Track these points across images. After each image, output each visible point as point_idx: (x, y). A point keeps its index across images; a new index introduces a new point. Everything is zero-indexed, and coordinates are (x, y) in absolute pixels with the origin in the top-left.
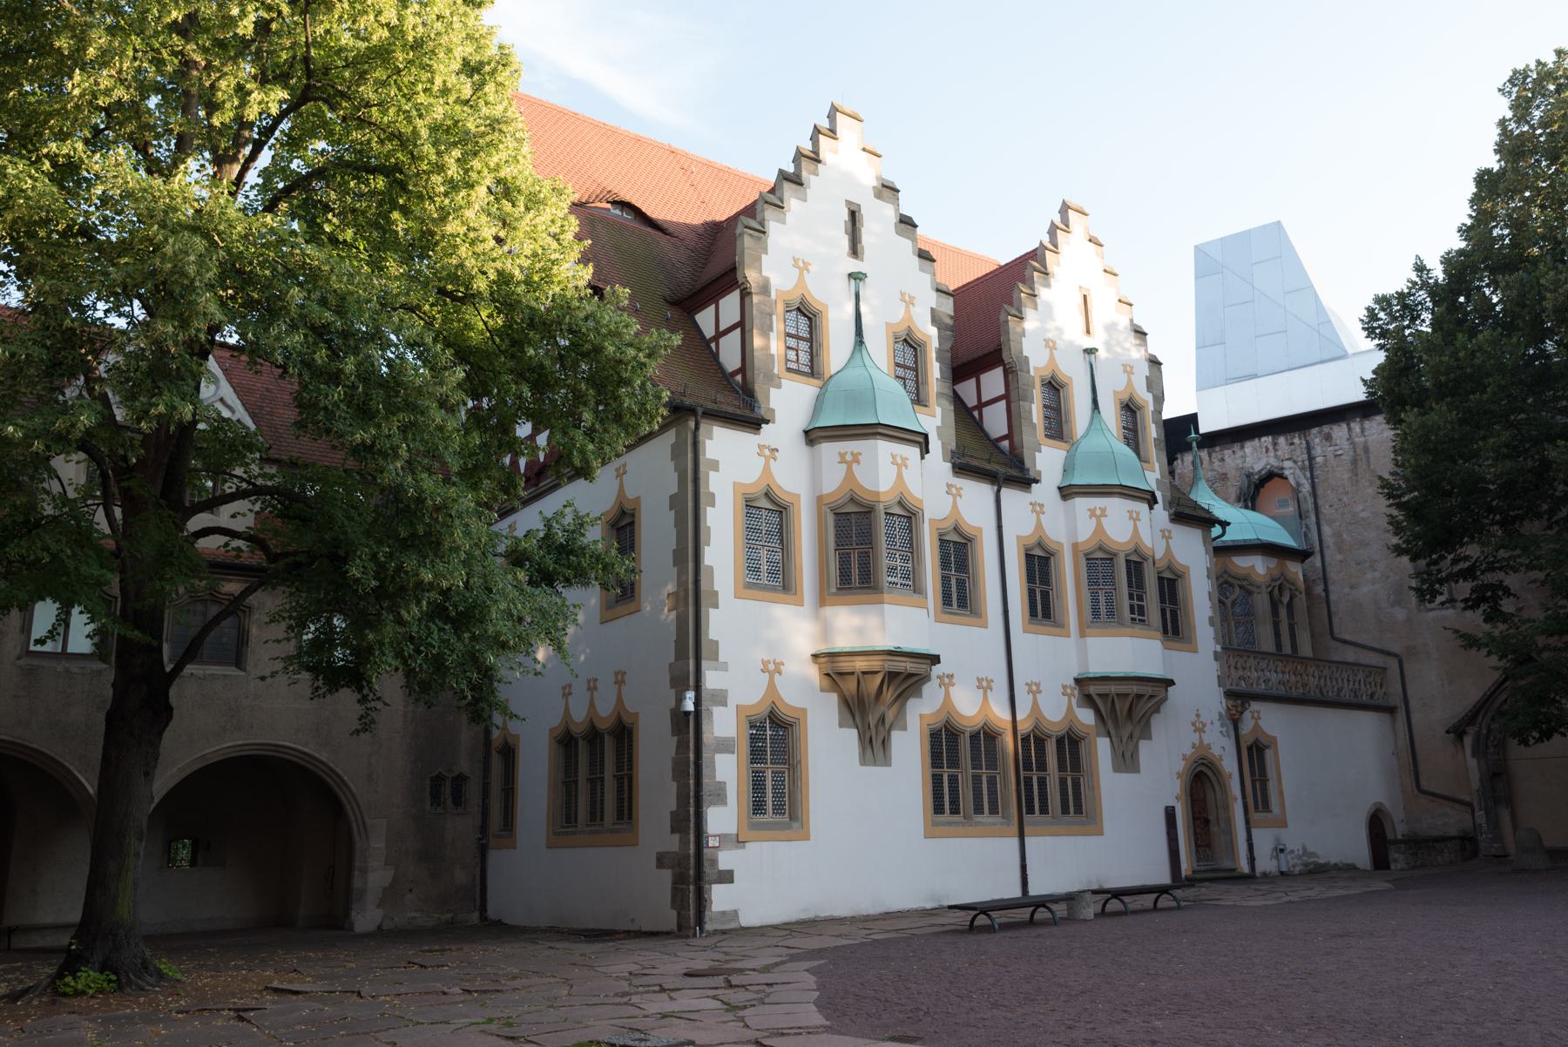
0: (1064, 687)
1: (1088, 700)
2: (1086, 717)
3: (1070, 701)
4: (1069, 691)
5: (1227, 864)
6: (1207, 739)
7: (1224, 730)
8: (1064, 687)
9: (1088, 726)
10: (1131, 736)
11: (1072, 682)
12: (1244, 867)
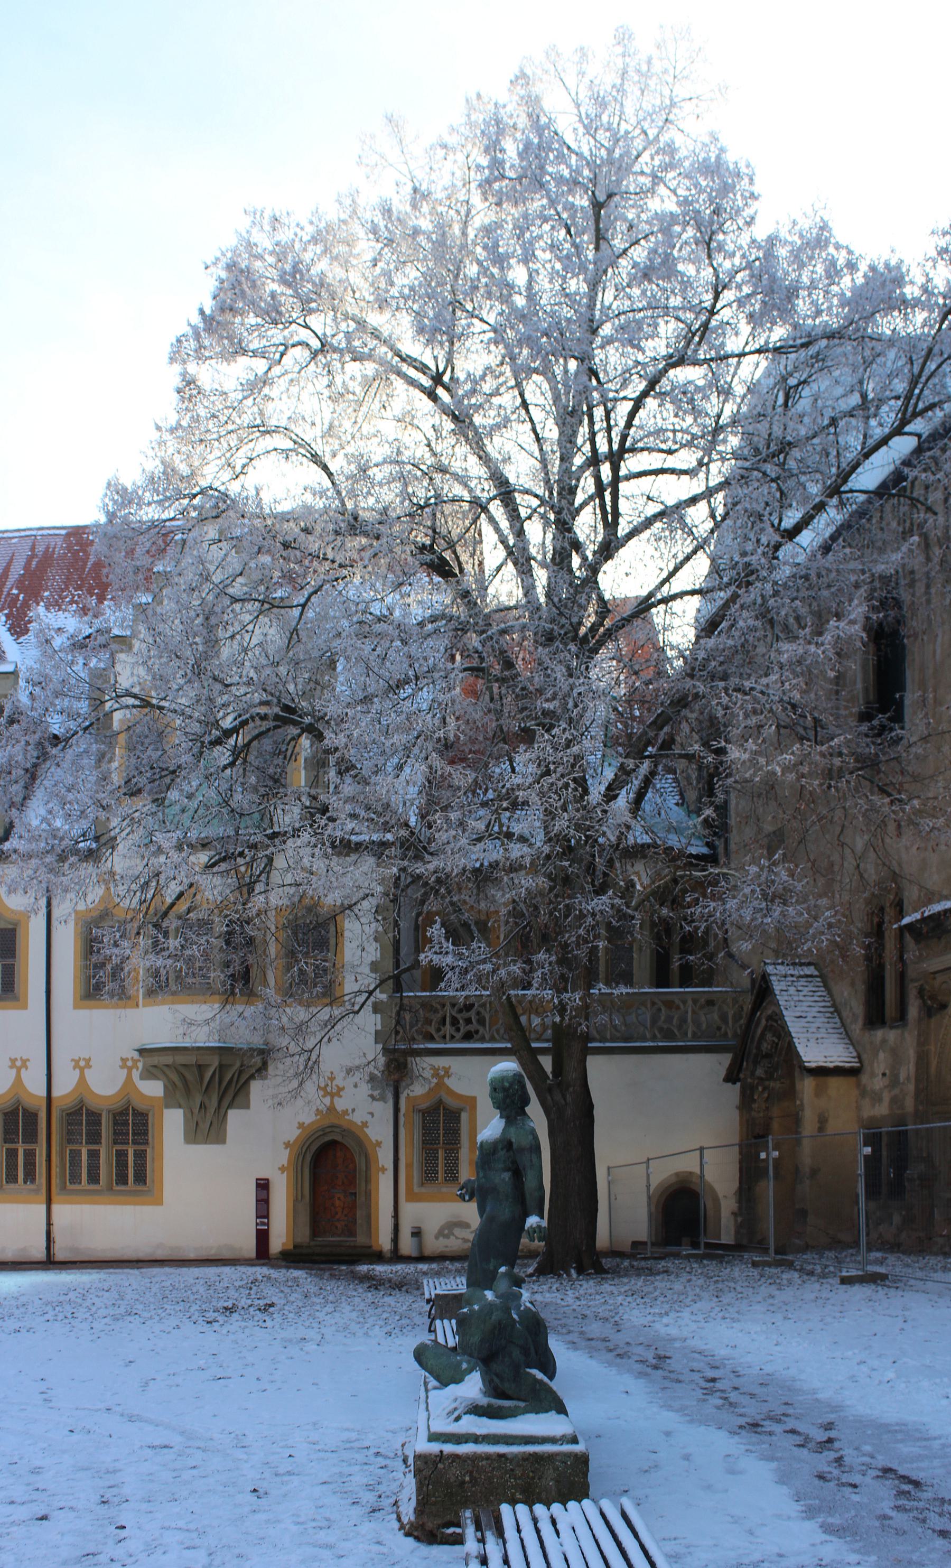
0: (124, 1060)
1: (149, 1074)
2: (154, 1089)
3: (129, 1075)
4: (130, 1063)
5: (361, 1239)
6: (341, 1104)
7: (376, 1093)
8: (124, 1060)
9: (152, 1098)
10: (202, 1106)
11: (136, 1055)
12: (384, 1242)
